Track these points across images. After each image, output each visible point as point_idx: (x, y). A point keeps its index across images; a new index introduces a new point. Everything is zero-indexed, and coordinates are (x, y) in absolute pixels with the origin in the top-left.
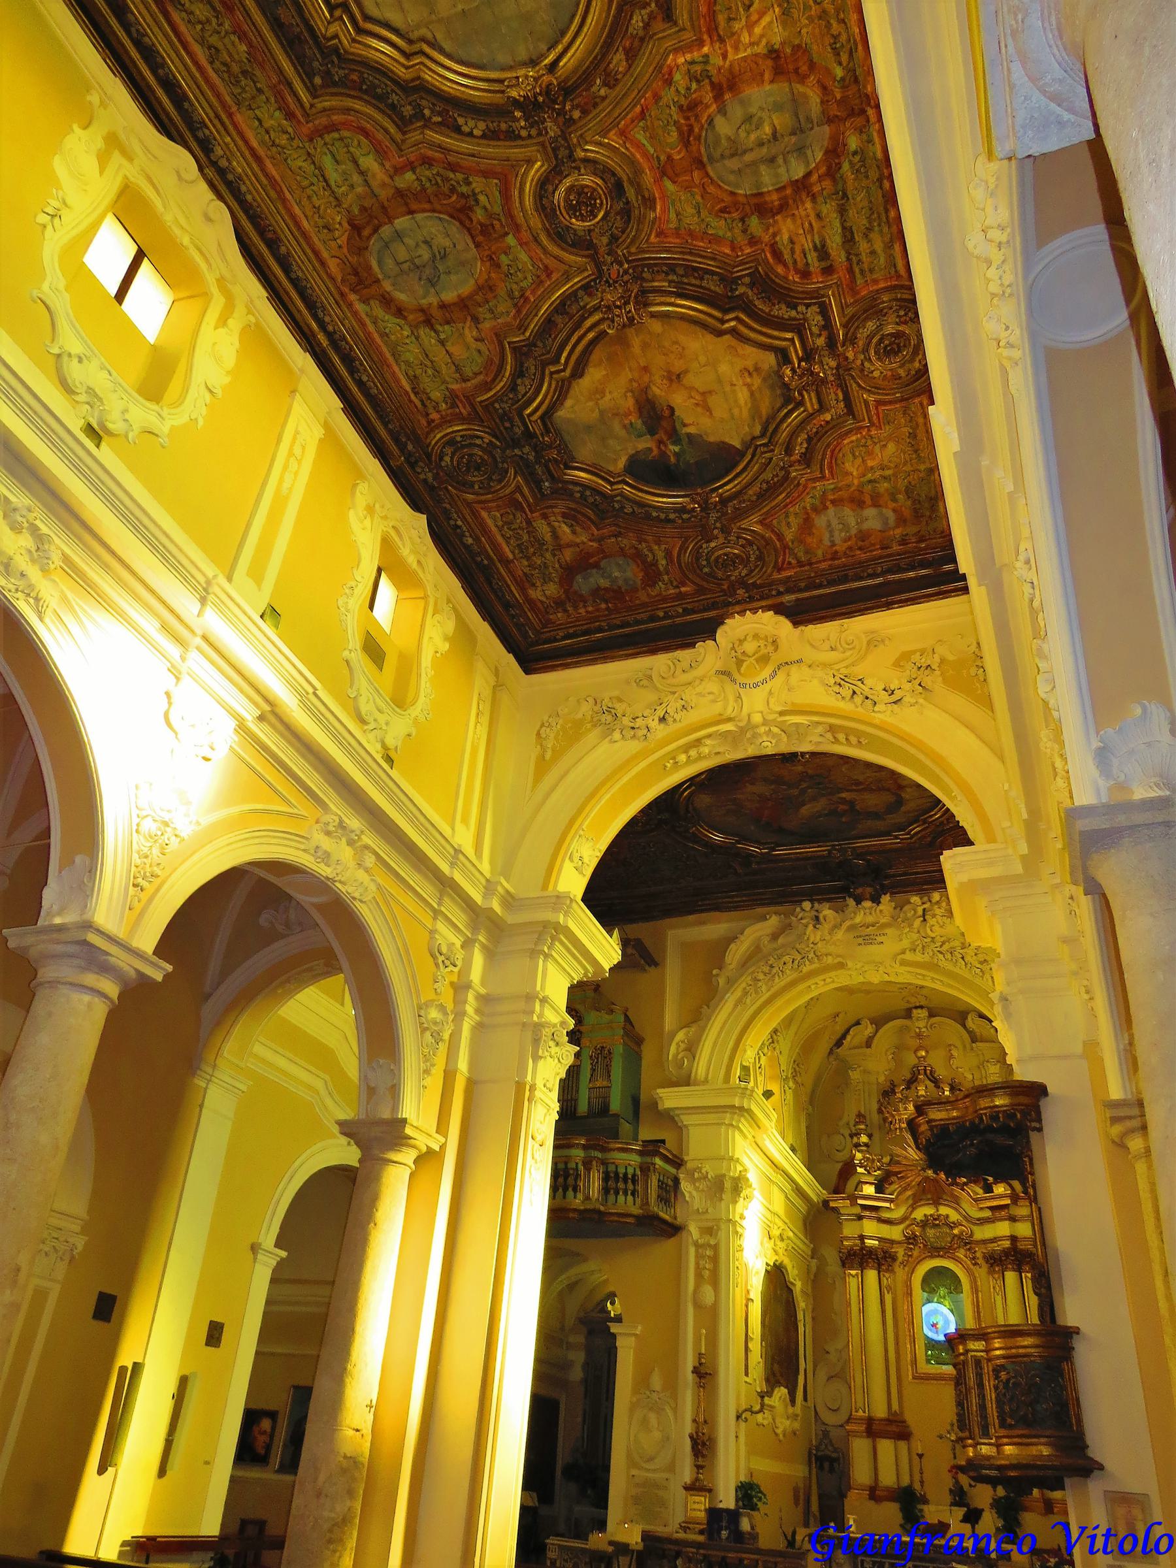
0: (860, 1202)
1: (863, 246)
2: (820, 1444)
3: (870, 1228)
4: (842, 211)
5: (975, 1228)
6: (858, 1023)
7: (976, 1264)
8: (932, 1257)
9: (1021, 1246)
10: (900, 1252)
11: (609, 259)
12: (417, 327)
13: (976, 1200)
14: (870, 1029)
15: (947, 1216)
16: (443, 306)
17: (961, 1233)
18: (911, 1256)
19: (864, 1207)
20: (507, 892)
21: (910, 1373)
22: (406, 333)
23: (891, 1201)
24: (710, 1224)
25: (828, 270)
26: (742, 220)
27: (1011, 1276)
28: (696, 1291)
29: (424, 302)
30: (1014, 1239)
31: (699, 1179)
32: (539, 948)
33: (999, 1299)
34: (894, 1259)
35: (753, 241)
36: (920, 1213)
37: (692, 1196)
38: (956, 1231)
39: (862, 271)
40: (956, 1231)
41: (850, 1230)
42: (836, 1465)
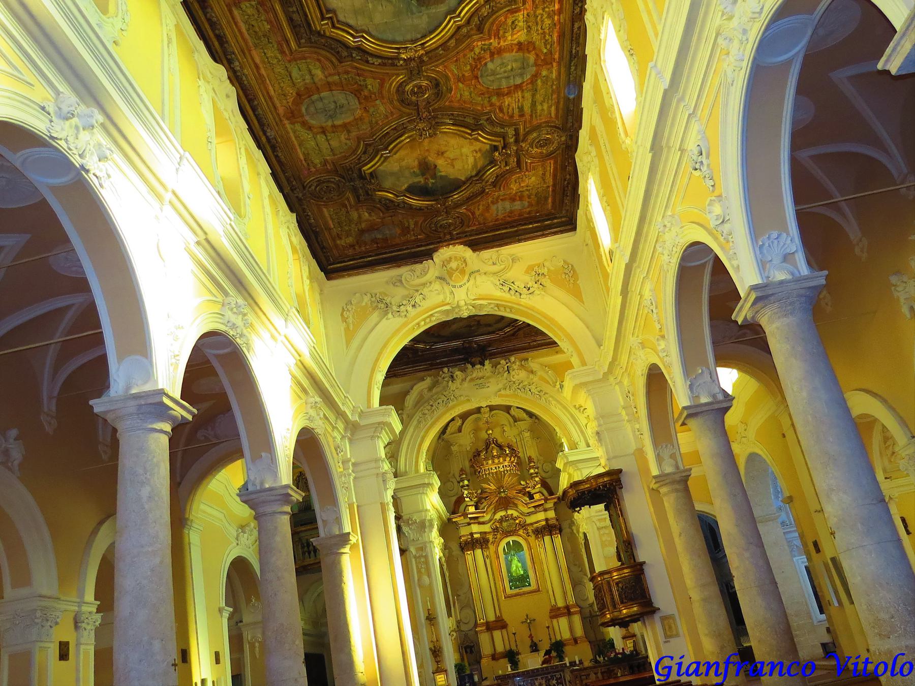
1: (539, 107)
3: (475, 528)
4: (533, 96)
5: (526, 518)
8: (507, 536)
10: (490, 537)
11: (423, 110)
12: (317, 133)
13: (526, 504)
15: (512, 514)
16: (333, 126)
17: (520, 522)
18: (496, 538)
20: (361, 410)
22: (310, 136)
23: (484, 512)
24: (421, 545)
25: (522, 115)
26: (489, 97)
28: (419, 580)
29: (324, 125)
31: (412, 524)
32: (375, 434)
35: (492, 105)
37: (409, 533)
38: (517, 521)
39: (536, 116)
40: (517, 521)
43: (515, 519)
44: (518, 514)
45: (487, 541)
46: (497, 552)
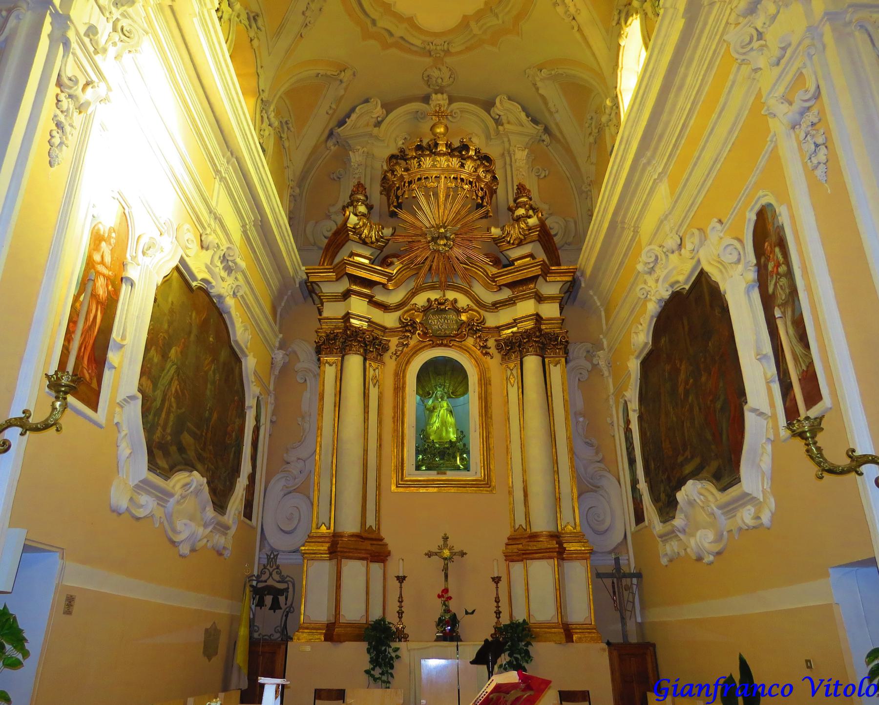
0: (351, 270)
2: (262, 573)
3: (358, 306)
6: (367, 101)
7: (487, 354)
8: (434, 345)
10: (394, 342)
14: (379, 111)
15: (455, 301)
19: (354, 279)
21: (394, 481)
27: (532, 362)
30: (538, 318)
33: (513, 392)
34: (386, 349)
36: (421, 300)
38: (464, 317)
40: (464, 317)
41: (332, 310)
42: (282, 599)
43: (458, 312)
44: (471, 304)
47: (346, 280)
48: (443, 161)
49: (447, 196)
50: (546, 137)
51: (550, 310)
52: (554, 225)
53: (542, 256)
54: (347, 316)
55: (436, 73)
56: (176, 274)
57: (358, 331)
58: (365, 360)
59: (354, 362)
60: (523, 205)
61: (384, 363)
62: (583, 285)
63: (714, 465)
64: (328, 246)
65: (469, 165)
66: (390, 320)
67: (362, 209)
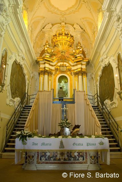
0: (46, 58)
3: (47, 65)
6: (49, 24)
7: (71, 75)
9: (83, 70)
10: (54, 72)
14: (51, 26)
15: (66, 65)
27: (80, 77)
30: (82, 68)
33: (77, 83)
34: (52, 74)
36: (59, 64)
40: (68, 68)
43: (66, 67)
45: (51, 74)
46: (55, 79)
47: (45, 60)
48: (64, 37)
49: (65, 44)
50: (84, 32)
51: (84, 67)
52: (85, 50)
53: (82, 56)
54: (45, 68)
55: (62, 19)
56: (14, 62)
57: (47, 70)
58: (48, 76)
59: (46, 76)
60: (79, 46)
61: (52, 76)
62: (90, 62)
63: (110, 97)
64: (41, 53)
65: (69, 38)
66: (53, 68)
67: (48, 46)
